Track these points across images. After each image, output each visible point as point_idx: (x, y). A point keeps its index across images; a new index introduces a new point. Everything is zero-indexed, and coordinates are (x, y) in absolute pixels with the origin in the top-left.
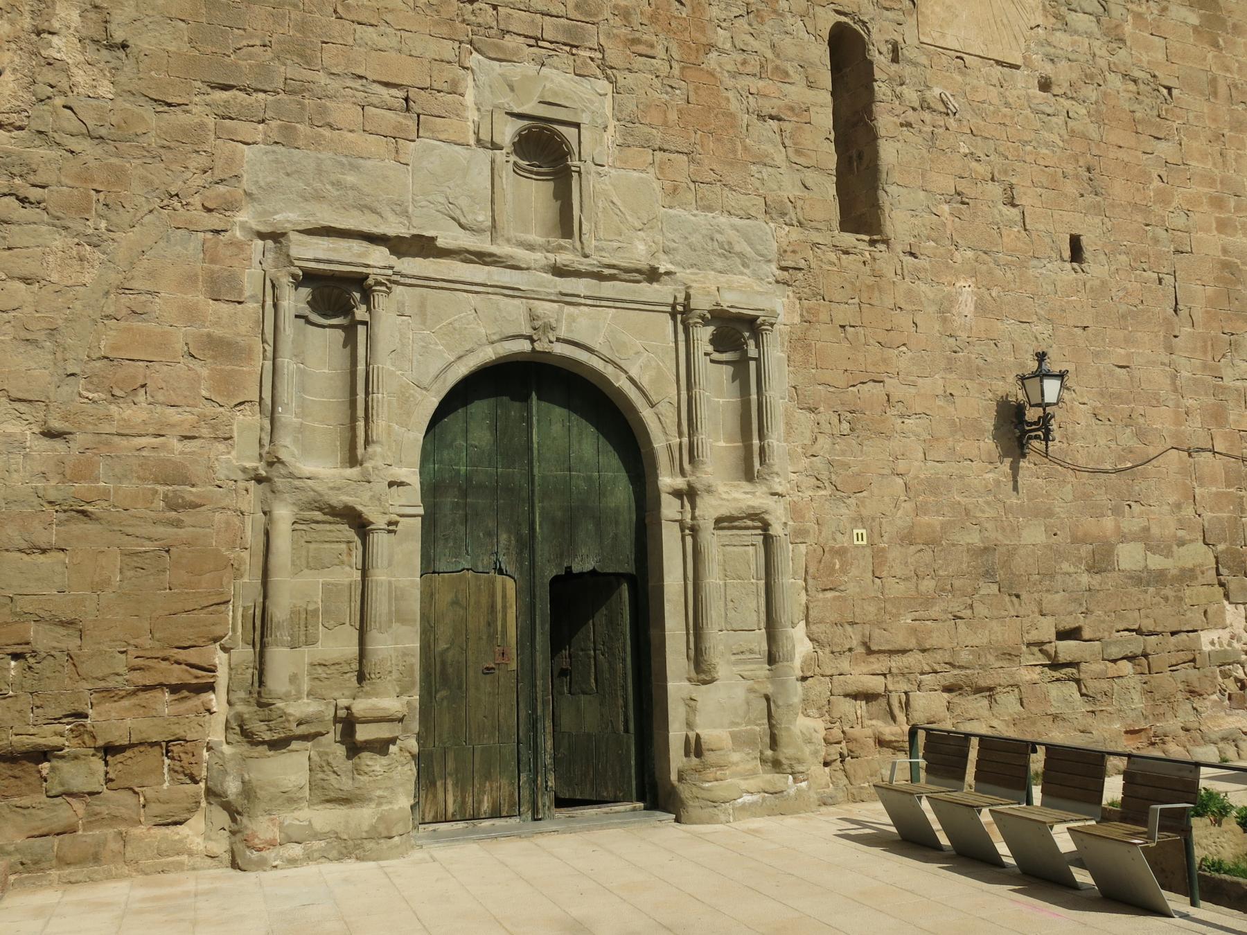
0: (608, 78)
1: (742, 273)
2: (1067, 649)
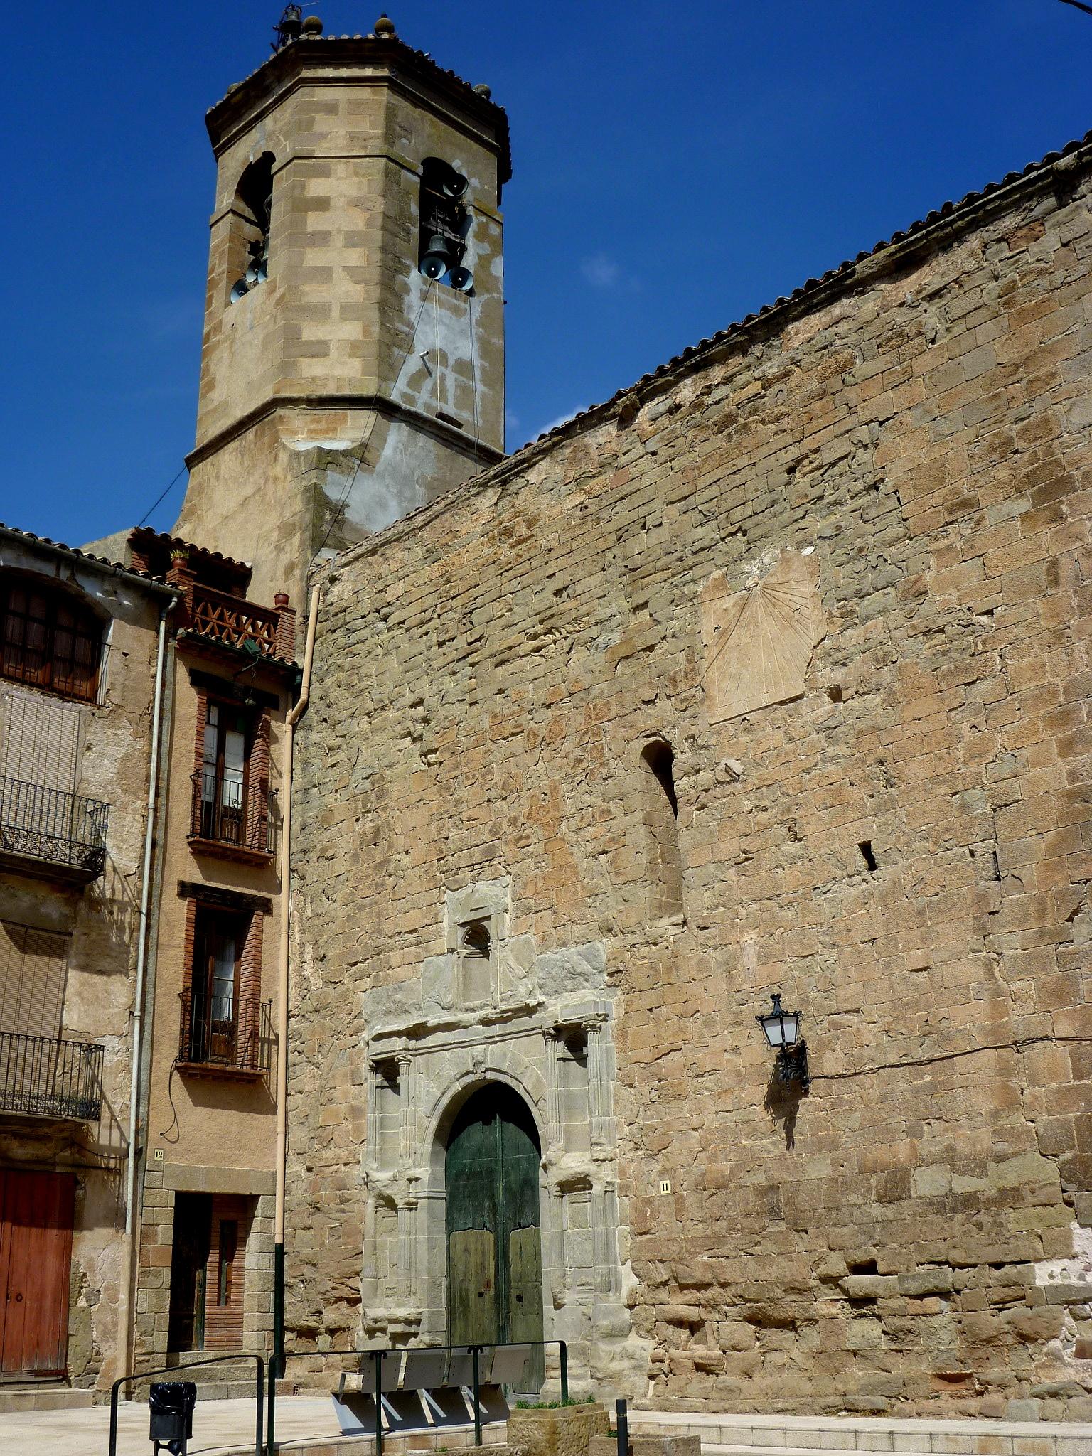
0: (509, 873)
1: (585, 988)
2: (861, 1283)
